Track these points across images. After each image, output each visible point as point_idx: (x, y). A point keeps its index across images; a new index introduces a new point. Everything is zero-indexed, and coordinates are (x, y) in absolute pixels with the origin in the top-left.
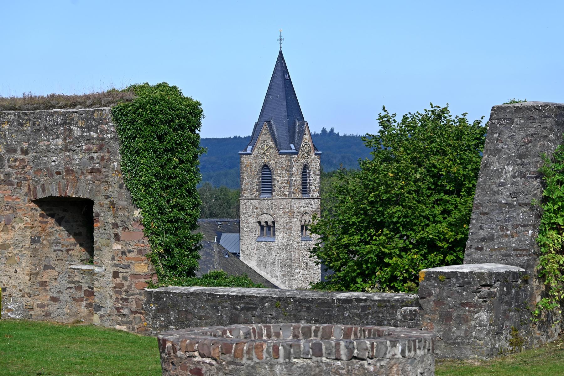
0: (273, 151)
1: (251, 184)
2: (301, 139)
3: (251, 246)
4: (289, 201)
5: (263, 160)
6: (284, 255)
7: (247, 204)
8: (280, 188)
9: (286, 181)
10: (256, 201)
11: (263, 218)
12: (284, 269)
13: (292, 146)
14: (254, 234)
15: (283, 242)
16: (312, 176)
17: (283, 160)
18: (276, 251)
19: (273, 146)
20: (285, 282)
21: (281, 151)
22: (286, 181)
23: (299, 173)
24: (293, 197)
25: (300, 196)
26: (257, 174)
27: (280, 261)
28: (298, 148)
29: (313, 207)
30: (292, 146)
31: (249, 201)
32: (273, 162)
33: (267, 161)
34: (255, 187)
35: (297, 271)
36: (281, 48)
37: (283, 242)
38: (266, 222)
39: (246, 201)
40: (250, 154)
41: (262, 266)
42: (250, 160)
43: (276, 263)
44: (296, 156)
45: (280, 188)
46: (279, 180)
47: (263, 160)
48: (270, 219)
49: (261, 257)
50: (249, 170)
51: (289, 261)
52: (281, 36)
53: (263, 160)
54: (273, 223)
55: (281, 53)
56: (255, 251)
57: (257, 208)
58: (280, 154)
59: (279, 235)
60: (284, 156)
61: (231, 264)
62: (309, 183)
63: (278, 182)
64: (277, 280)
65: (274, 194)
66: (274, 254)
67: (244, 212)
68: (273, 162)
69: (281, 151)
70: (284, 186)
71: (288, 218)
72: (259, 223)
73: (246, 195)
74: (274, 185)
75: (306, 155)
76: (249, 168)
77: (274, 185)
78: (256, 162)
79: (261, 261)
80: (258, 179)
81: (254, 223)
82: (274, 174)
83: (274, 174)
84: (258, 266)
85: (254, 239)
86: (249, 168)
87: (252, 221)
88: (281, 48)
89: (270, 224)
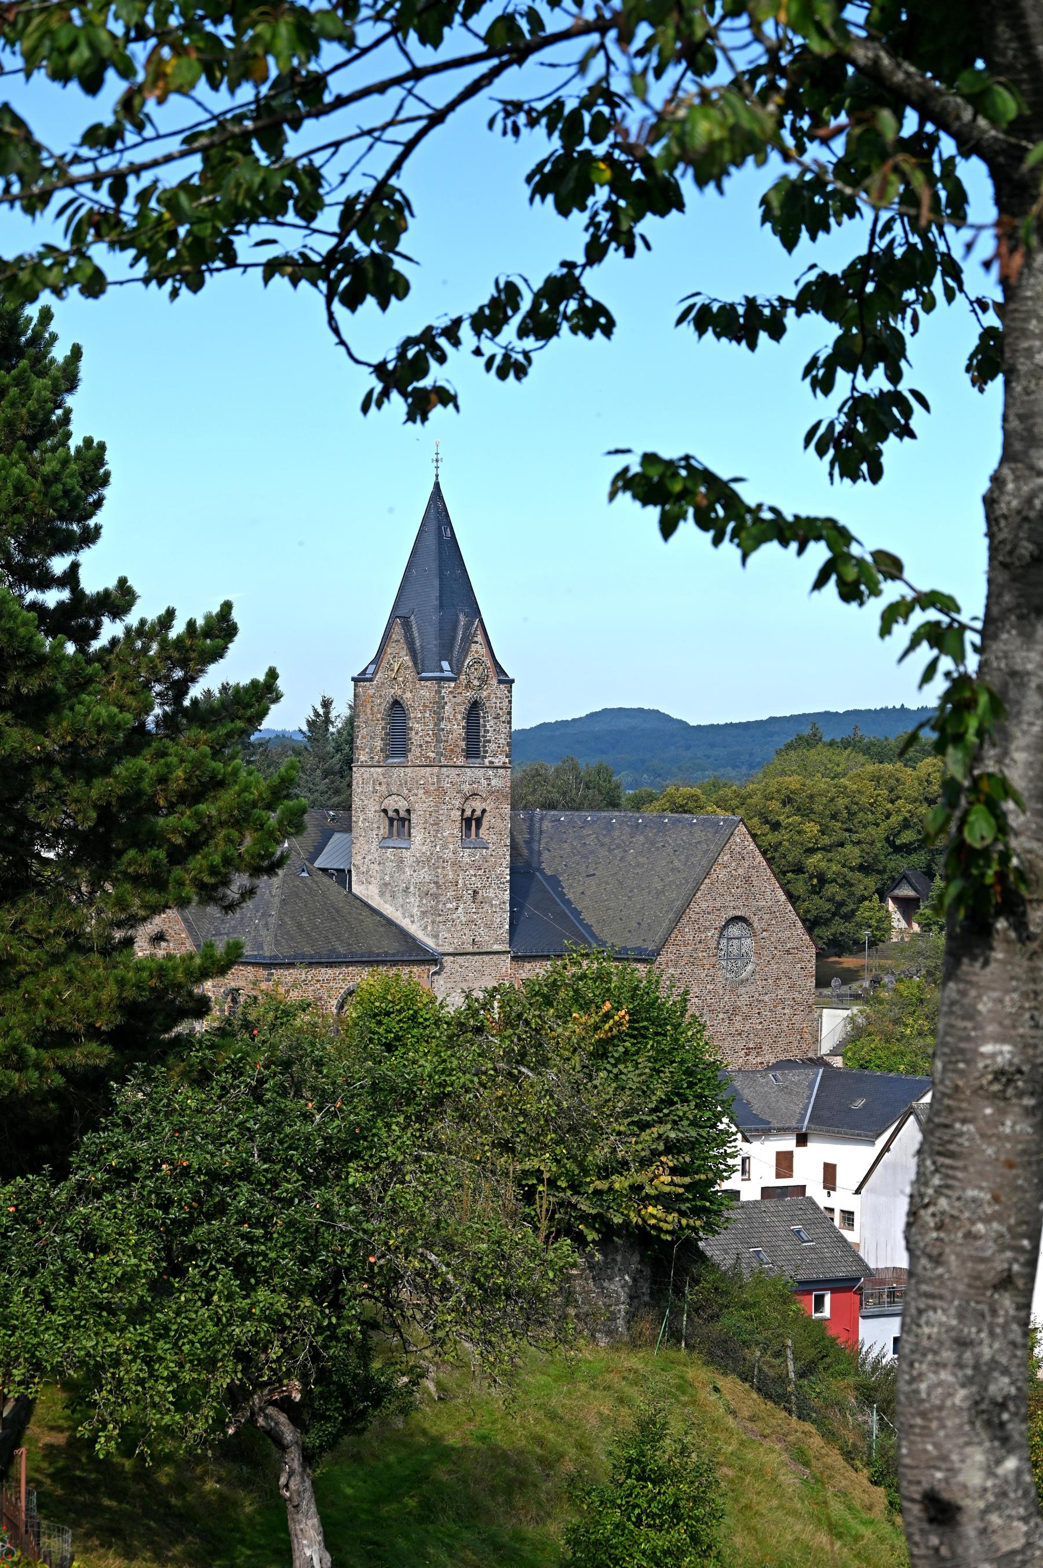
0: (410, 674)
2: (465, 651)
4: (436, 770)
6: (424, 874)
11: (391, 803)
13: (445, 665)
17: (426, 692)
23: (459, 717)
24: (444, 762)
25: (461, 761)
27: (419, 885)
28: (457, 669)
30: (445, 665)
32: (408, 695)
34: (379, 744)
38: (397, 811)
40: (371, 680)
42: (371, 692)
46: (419, 730)
48: (402, 805)
54: (408, 811)
55: (437, 485)
56: (376, 867)
58: (421, 679)
59: (418, 835)
65: (410, 756)
66: (408, 871)
68: (408, 695)
72: (385, 811)
73: (362, 758)
75: (476, 683)
79: (386, 885)
84: (382, 894)
89: (402, 814)
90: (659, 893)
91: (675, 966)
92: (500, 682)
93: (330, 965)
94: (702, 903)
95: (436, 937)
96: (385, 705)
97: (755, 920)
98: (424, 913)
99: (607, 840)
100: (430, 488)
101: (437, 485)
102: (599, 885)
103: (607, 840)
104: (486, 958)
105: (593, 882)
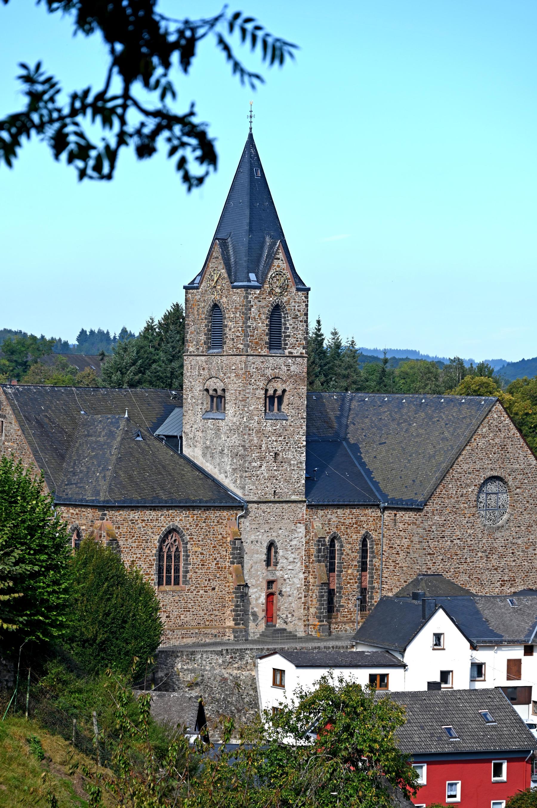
0: (225, 283)
1: (198, 333)
2: (269, 266)
3: (196, 426)
4: (244, 358)
5: (213, 297)
7: (193, 364)
8: (233, 339)
9: (240, 329)
10: (203, 358)
11: (212, 384)
12: (235, 461)
13: (252, 276)
14: (200, 407)
15: (235, 420)
16: (291, 322)
17: (237, 297)
18: (226, 433)
19: (226, 275)
20: (236, 481)
21: (235, 284)
22: (240, 329)
23: (263, 317)
24: (250, 351)
25: (265, 352)
26: (206, 319)
28: (262, 280)
29: (292, 368)
30: (252, 276)
31: (195, 358)
32: (224, 300)
33: (218, 298)
34: (203, 338)
35: (254, 464)
36: (251, 129)
37: (235, 420)
39: (191, 358)
40: (197, 288)
41: (208, 455)
43: (226, 451)
44: (258, 292)
45: (233, 339)
46: (232, 327)
47: (213, 297)
48: (220, 385)
49: (208, 443)
50: (196, 313)
51: (241, 448)
52: (251, 111)
53: (212, 297)
55: (251, 136)
57: (204, 369)
58: (234, 287)
59: (230, 409)
60: (239, 291)
61: (143, 450)
62: (285, 332)
63: (230, 330)
64: (226, 477)
67: (188, 374)
68: (224, 300)
69: (235, 284)
70: (238, 336)
71: (241, 384)
73: (191, 349)
74: (225, 334)
75: (278, 290)
76: (196, 309)
77: (225, 334)
78: (204, 300)
79: (207, 448)
80: (206, 326)
81: (200, 391)
82: (225, 318)
83: (225, 318)
84: (204, 455)
85: (199, 416)
86: (196, 309)
87: (198, 388)
88: (251, 129)
90: (431, 457)
91: (440, 514)
92: (298, 290)
93: (154, 508)
94: (464, 465)
95: (243, 488)
96: (208, 308)
97: (510, 480)
98: (234, 470)
99: (397, 416)
100: (246, 138)
101: (251, 136)
102: (387, 451)
103: (397, 416)
104: (286, 506)
105: (383, 448)
